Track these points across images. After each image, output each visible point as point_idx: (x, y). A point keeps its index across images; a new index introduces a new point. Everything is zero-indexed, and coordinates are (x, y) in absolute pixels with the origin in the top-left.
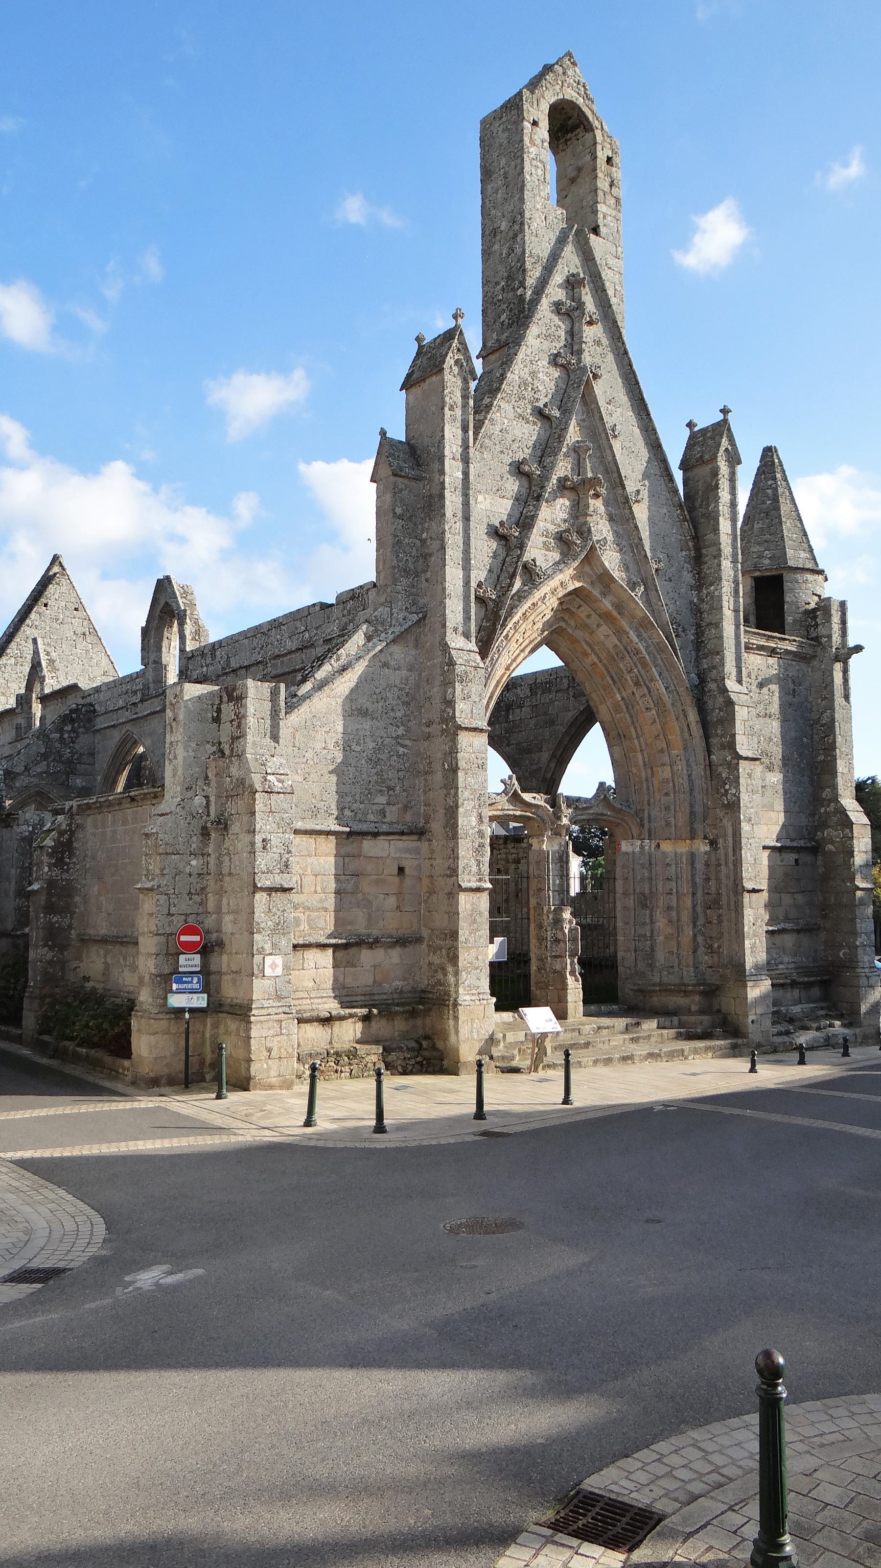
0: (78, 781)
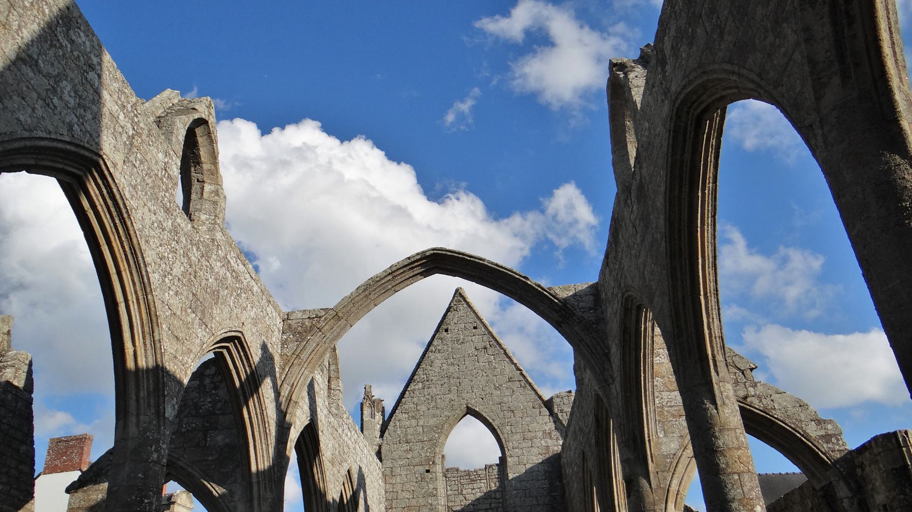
0: (220, 438)
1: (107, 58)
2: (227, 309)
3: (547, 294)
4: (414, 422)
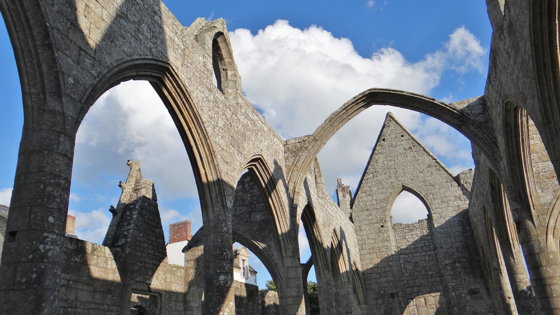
0: (258, 217)
1: (163, 5)
2: (251, 143)
3: (448, 108)
4: (370, 198)
